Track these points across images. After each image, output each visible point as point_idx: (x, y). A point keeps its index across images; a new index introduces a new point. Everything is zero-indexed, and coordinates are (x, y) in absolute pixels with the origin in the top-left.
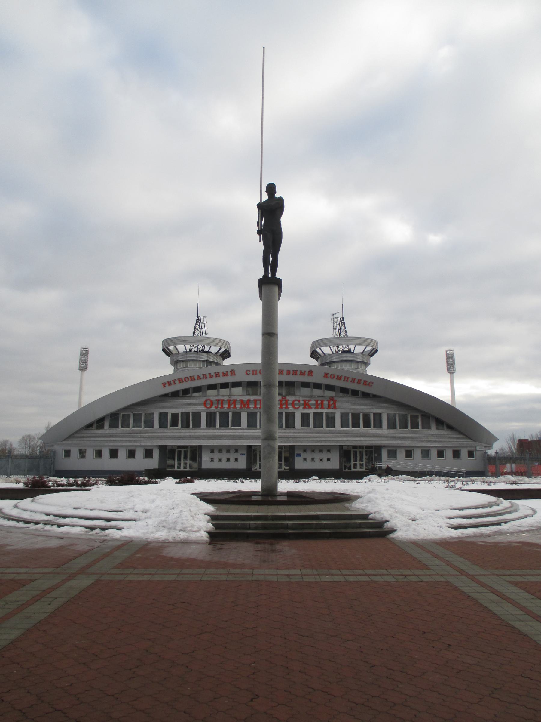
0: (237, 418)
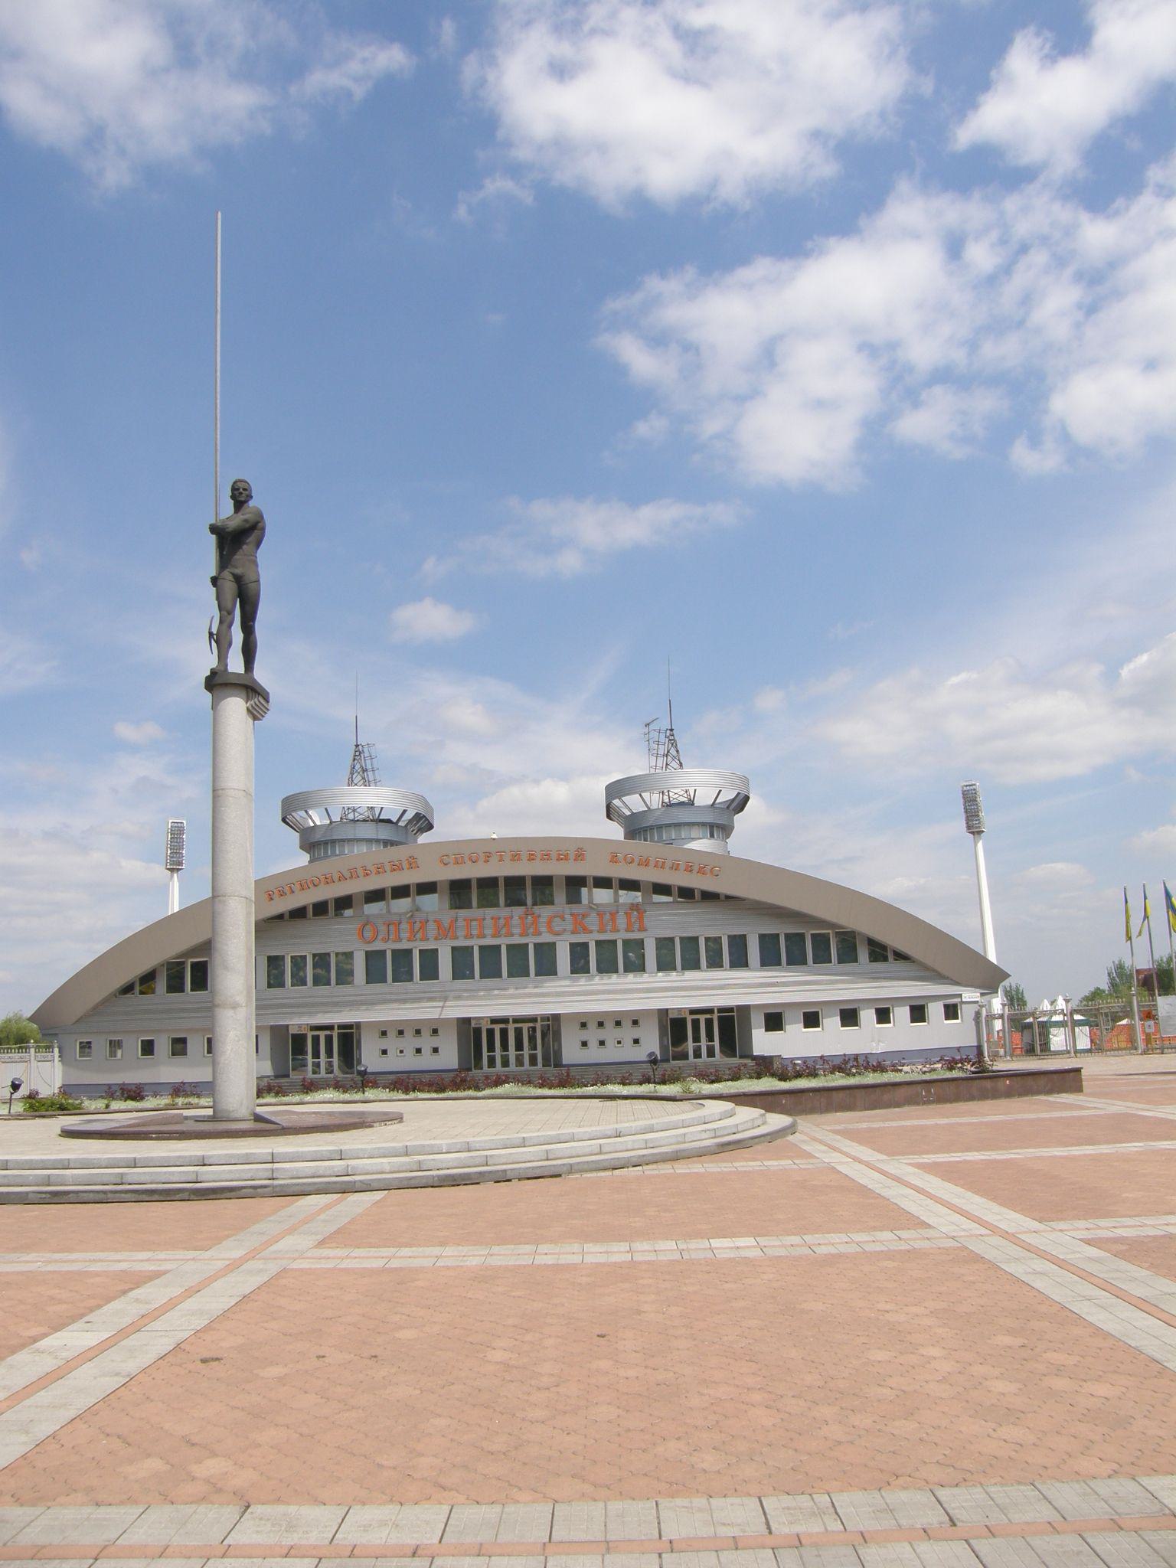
0: (430, 960)
